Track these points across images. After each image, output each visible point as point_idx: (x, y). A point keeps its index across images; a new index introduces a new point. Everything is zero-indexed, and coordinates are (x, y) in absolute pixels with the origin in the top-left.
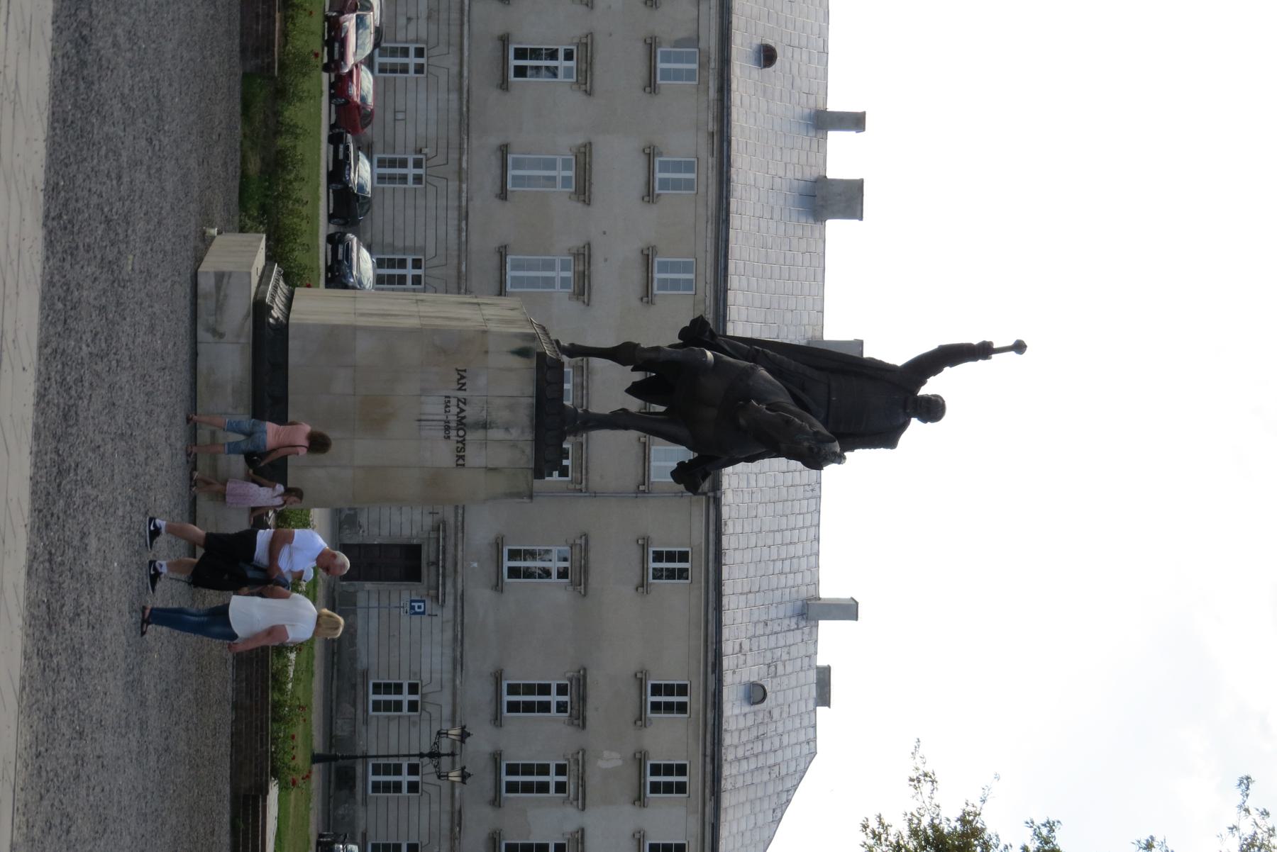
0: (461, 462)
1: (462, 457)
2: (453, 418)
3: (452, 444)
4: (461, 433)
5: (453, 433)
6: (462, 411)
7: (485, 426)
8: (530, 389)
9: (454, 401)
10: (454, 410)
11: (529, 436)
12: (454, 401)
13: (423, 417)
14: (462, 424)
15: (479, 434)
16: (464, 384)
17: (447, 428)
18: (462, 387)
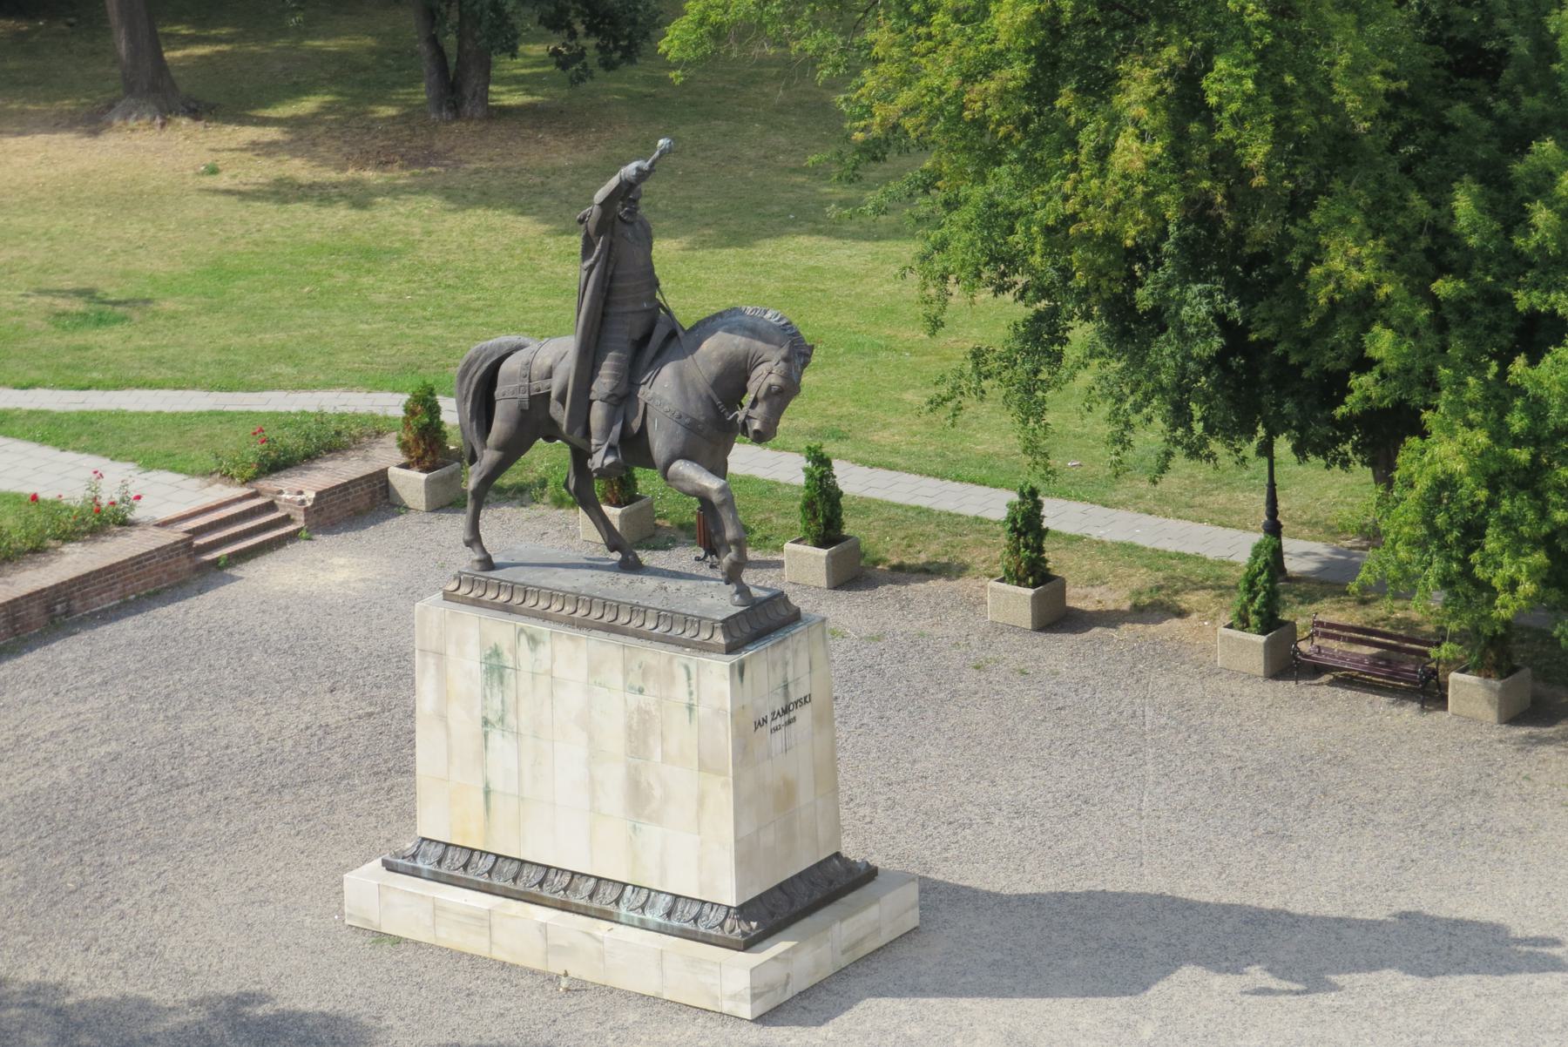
2: (780, 721)
7: (786, 687)
9: (774, 724)
15: (791, 688)
17: (790, 722)
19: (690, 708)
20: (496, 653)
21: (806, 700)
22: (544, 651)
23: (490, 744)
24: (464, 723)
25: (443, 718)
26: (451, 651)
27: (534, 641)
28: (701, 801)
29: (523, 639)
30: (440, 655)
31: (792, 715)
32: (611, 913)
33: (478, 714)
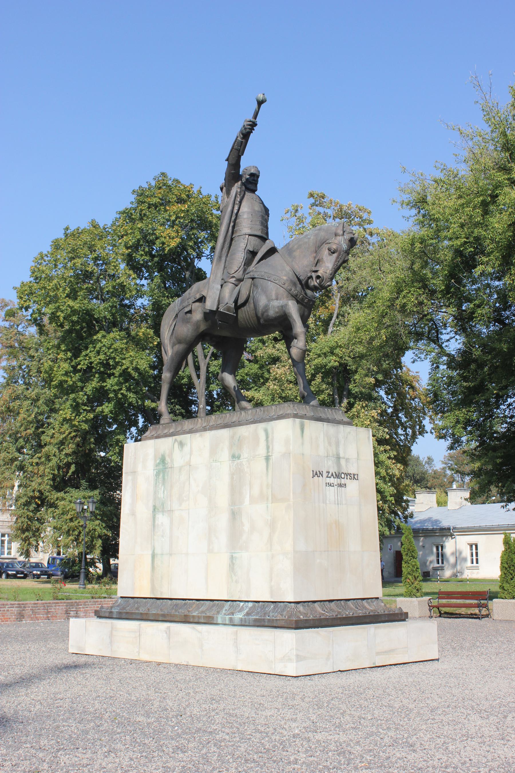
0: (356, 477)
1: (354, 475)
2: (335, 481)
3: (347, 481)
4: (343, 476)
5: (343, 481)
6: (332, 475)
7: (338, 458)
8: (319, 424)
9: (328, 480)
10: (332, 480)
11: (341, 427)
12: (328, 480)
13: (336, 502)
14: (338, 476)
15: (343, 462)
16: (320, 473)
17: (340, 485)
18: (321, 474)
19: (267, 458)
20: (163, 460)
21: (354, 477)
22: (187, 449)
23: (157, 522)
24: (143, 511)
25: (133, 514)
26: (140, 468)
27: (181, 444)
28: (272, 525)
29: (176, 445)
30: (134, 472)
31: (343, 481)
32: (212, 618)
33: (151, 504)
